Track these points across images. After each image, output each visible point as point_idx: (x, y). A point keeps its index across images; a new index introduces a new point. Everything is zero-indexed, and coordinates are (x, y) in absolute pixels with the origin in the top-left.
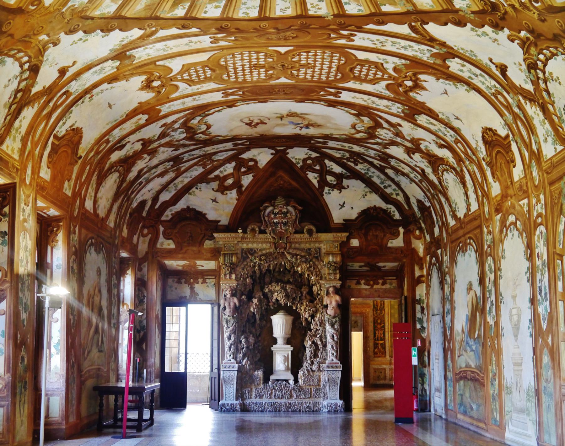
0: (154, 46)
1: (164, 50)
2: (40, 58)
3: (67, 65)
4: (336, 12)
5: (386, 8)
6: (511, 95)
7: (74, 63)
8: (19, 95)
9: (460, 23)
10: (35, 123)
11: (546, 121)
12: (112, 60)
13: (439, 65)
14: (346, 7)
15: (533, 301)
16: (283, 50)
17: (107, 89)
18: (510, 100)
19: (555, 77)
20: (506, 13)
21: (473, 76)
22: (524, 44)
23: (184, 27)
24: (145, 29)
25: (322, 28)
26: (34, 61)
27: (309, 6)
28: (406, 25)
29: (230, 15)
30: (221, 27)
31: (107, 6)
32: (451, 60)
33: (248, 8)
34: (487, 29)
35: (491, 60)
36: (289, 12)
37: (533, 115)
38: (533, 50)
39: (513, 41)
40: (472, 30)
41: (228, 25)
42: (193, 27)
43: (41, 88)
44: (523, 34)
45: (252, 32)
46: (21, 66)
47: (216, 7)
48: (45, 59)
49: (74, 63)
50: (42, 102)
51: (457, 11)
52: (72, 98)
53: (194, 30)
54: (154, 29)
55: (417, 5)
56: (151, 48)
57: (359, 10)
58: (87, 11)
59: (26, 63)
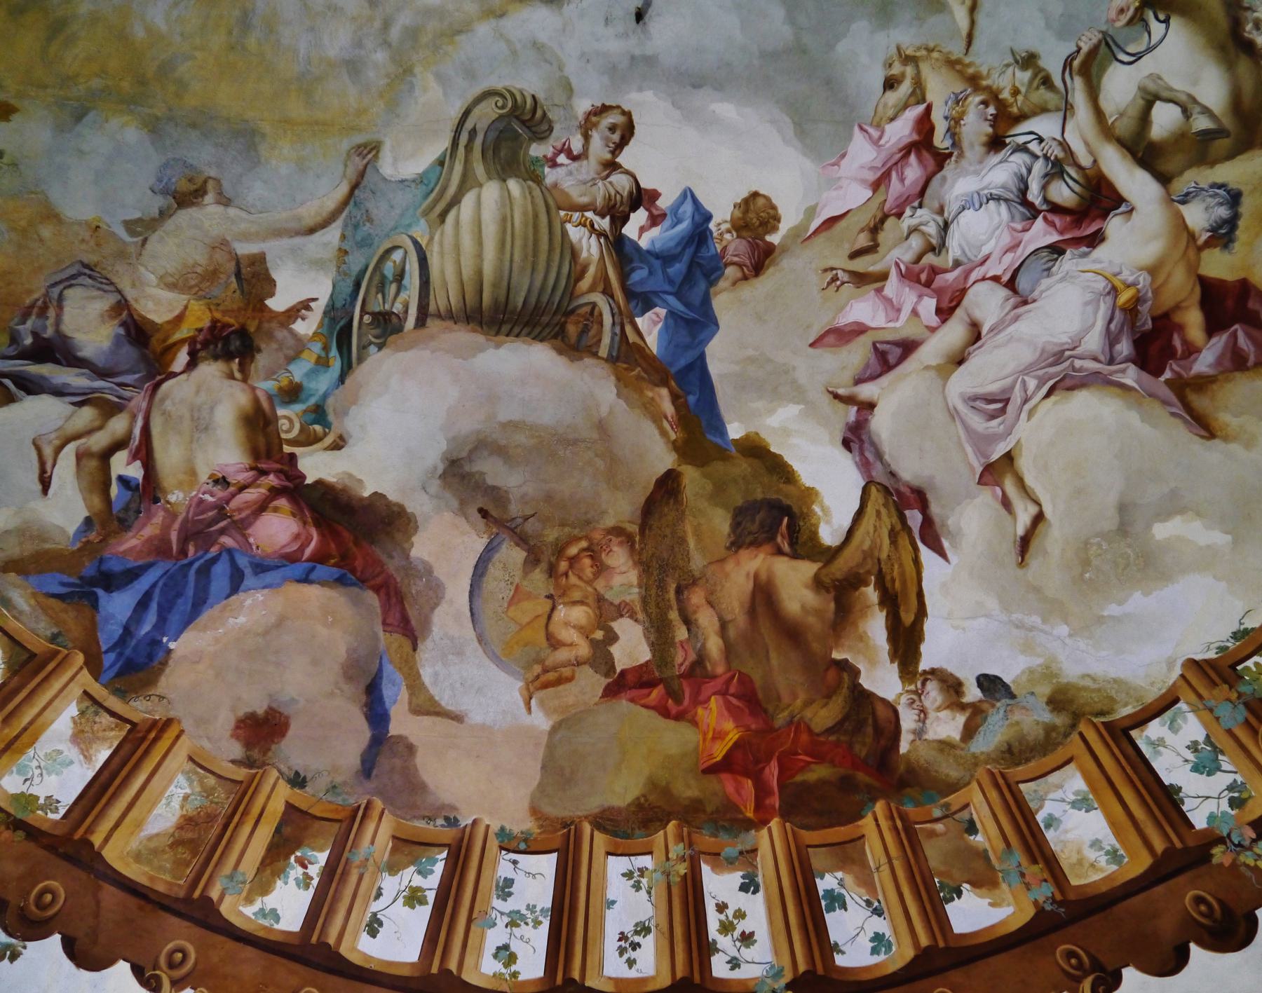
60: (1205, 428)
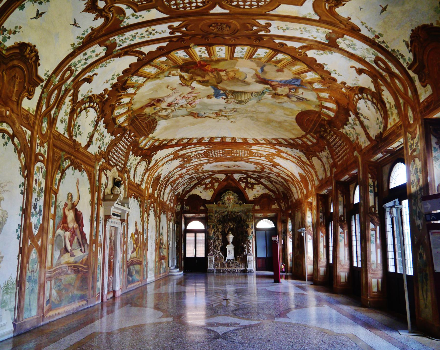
0: (309, 37)
1: (305, 29)
2: (354, 89)
3: (355, 71)
4: (189, 49)
5: (164, 59)
6: (72, 83)
7: (352, 67)
8: (375, 101)
9: (125, 72)
10: (393, 90)
11: (68, 116)
12: (338, 46)
13: (105, 40)
14: (185, 54)
15: (25, 211)
16: (218, 10)
17: (366, 27)
18: (69, 82)
19: (88, 114)
20: (119, 92)
21: (86, 57)
22: (102, 95)
23: (282, 45)
24: (304, 53)
25: (193, 36)
26: (357, 92)
27: (206, 52)
28: (146, 53)
29: (252, 48)
30: (260, 41)
31: (310, 76)
32: (105, 51)
33: (241, 52)
34: (115, 81)
35: (96, 74)
36: (217, 48)
37: (66, 104)
38: (98, 100)
39: (104, 90)
40: (118, 75)
41: (255, 42)
42: (277, 44)
43: (372, 84)
44: (107, 96)
45: (240, 36)
46: (360, 99)
47: (259, 55)
48: (355, 86)
49: (352, 67)
50: (381, 83)
51: (133, 75)
52: (380, 55)
53: (277, 41)
54: (300, 51)
55: (151, 67)
56: (312, 36)
57: (177, 53)
58: (320, 81)
59: (358, 96)
60: (150, 99)
